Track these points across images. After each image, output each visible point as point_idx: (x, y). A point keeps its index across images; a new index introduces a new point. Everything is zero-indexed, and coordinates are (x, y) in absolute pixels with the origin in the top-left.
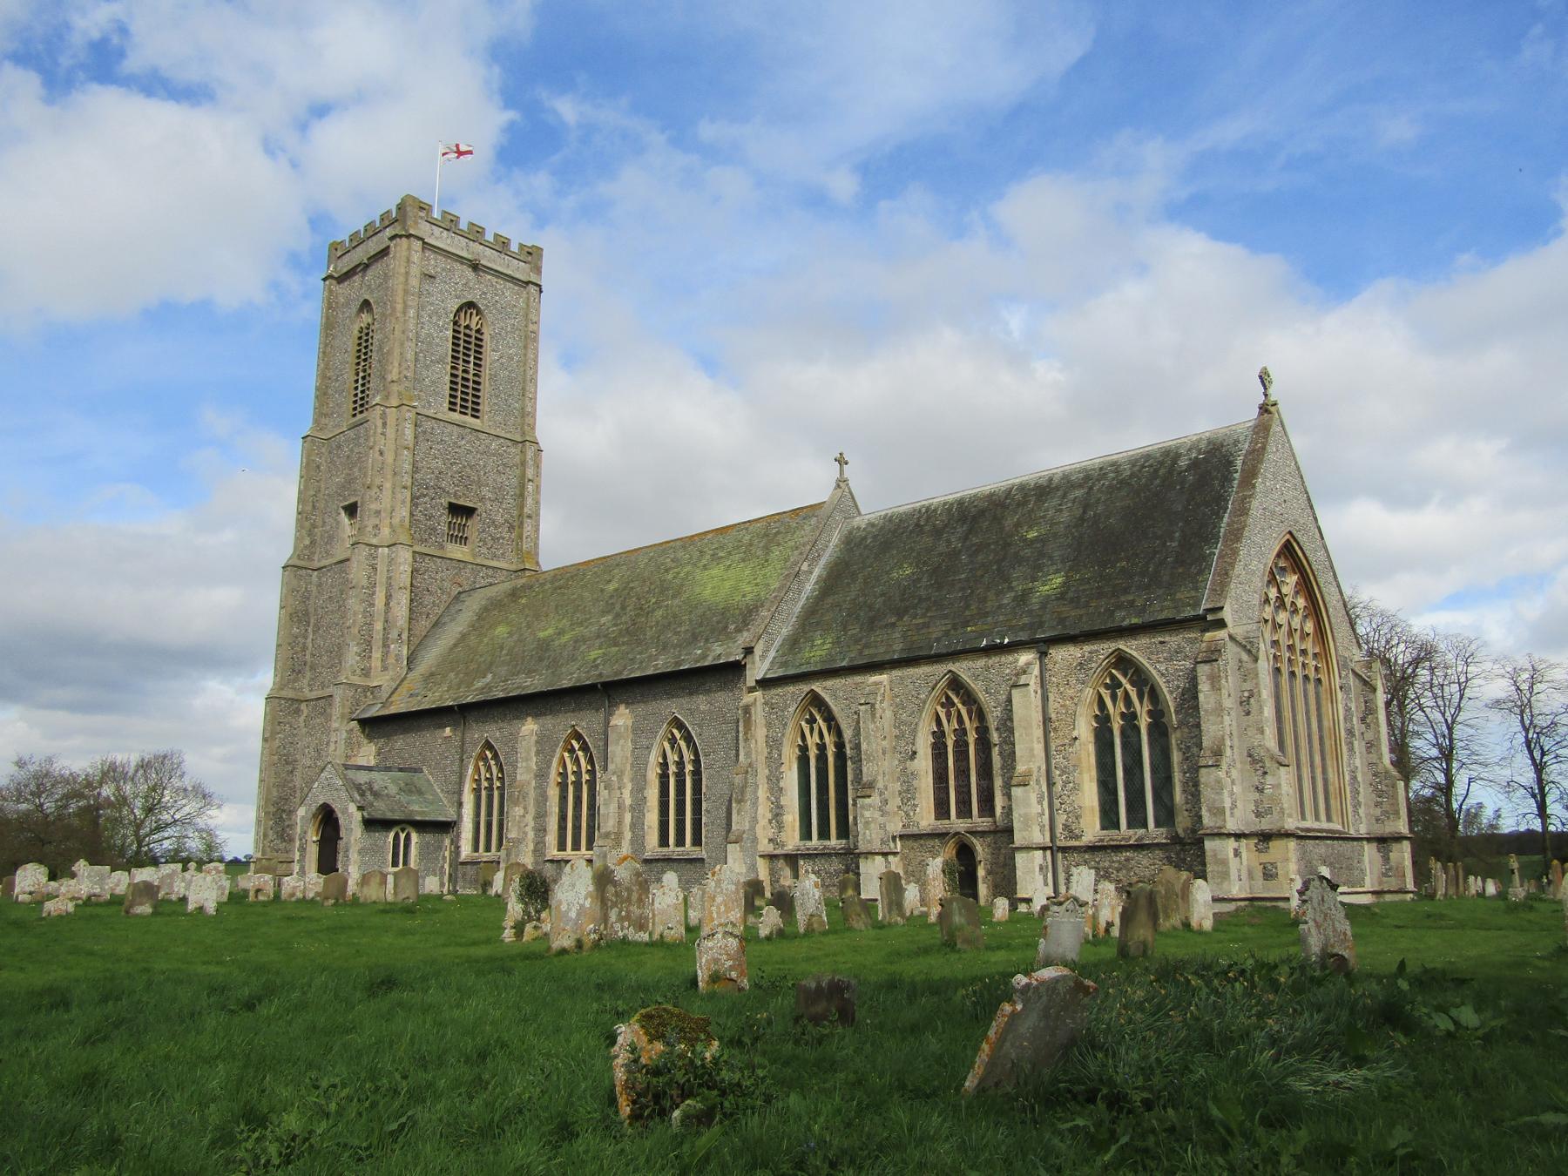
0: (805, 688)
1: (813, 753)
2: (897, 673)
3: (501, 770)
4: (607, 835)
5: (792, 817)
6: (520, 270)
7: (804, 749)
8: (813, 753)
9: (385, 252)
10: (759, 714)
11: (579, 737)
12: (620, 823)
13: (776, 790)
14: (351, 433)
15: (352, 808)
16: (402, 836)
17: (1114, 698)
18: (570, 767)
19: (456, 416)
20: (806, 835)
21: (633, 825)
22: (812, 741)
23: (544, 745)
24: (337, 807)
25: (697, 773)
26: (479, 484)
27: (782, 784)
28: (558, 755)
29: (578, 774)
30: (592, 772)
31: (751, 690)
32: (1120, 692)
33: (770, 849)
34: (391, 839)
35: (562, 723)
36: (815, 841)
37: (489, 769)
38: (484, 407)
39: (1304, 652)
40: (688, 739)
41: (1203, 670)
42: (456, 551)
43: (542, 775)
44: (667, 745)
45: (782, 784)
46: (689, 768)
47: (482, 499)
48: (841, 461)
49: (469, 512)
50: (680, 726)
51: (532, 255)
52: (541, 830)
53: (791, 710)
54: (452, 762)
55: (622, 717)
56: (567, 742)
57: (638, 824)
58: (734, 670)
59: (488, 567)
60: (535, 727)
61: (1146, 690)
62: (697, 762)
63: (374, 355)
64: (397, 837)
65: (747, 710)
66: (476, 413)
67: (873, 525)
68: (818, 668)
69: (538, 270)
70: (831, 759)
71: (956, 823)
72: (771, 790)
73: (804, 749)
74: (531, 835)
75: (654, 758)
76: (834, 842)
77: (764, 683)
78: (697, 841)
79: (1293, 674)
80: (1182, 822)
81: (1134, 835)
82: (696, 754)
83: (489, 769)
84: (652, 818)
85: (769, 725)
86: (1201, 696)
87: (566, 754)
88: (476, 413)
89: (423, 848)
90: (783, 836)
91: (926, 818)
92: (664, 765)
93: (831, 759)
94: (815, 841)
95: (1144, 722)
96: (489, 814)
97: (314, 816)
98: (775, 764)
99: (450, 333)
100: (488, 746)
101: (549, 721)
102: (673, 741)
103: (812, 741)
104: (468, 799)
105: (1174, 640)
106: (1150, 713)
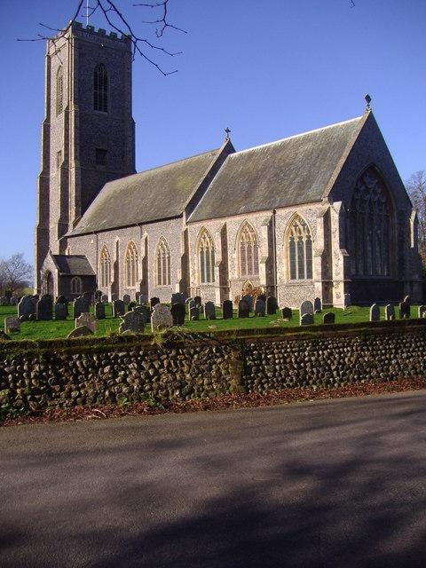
15: (57, 271)
19: (97, 112)
20: (203, 281)
38: (109, 107)
42: (102, 167)
66: (106, 110)
78: (169, 283)
99: (92, 78)
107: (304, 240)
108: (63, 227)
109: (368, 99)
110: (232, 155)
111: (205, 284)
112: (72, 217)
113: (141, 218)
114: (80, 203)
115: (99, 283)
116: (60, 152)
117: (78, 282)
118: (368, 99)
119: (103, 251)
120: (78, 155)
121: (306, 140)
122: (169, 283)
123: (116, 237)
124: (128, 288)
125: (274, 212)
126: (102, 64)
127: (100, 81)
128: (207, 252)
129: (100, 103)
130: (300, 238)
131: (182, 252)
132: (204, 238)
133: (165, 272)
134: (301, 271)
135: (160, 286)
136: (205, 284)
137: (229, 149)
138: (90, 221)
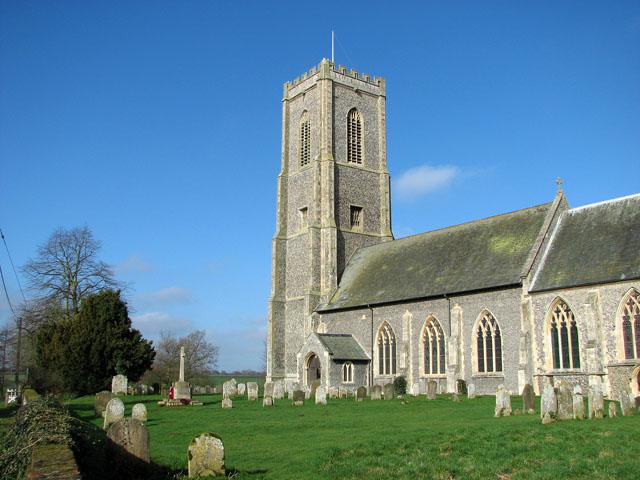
0: (554, 295)
1: (559, 327)
2: (604, 287)
4: (453, 366)
7: (554, 325)
8: (559, 327)
10: (531, 308)
12: (459, 360)
13: (541, 345)
15: (326, 354)
16: (348, 367)
18: (430, 334)
19: (351, 163)
20: (557, 365)
22: (559, 322)
23: (416, 323)
24: (318, 353)
25: (498, 336)
30: (442, 337)
31: (525, 296)
33: (537, 372)
36: (562, 369)
37: (386, 335)
38: (363, 158)
40: (493, 321)
43: (416, 338)
46: (493, 335)
49: (359, 209)
52: (416, 364)
56: (428, 322)
58: (519, 285)
65: (525, 306)
68: (561, 285)
70: (559, 331)
73: (554, 325)
74: (411, 366)
75: (475, 330)
76: (571, 369)
83: (386, 335)
84: (475, 358)
85: (536, 314)
87: (428, 329)
89: (357, 372)
90: (545, 367)
92: (480, 333)
93: (559, 331)
94: (562, 369)
96: (388, 356)
97: (306, 357)
98: (539, 331)
100: (386, 324)
101: (418, 313)
102: (484, 322)
103: (559, 322)
108: (315, 298)
113: (448, 288)
114: (336, 271)
116: (304, 210)
122: (499, 368)
123: (407, 314)
126: (354, 109)
128: (564, 329)
129: (353, 153)
135: (482, 373)
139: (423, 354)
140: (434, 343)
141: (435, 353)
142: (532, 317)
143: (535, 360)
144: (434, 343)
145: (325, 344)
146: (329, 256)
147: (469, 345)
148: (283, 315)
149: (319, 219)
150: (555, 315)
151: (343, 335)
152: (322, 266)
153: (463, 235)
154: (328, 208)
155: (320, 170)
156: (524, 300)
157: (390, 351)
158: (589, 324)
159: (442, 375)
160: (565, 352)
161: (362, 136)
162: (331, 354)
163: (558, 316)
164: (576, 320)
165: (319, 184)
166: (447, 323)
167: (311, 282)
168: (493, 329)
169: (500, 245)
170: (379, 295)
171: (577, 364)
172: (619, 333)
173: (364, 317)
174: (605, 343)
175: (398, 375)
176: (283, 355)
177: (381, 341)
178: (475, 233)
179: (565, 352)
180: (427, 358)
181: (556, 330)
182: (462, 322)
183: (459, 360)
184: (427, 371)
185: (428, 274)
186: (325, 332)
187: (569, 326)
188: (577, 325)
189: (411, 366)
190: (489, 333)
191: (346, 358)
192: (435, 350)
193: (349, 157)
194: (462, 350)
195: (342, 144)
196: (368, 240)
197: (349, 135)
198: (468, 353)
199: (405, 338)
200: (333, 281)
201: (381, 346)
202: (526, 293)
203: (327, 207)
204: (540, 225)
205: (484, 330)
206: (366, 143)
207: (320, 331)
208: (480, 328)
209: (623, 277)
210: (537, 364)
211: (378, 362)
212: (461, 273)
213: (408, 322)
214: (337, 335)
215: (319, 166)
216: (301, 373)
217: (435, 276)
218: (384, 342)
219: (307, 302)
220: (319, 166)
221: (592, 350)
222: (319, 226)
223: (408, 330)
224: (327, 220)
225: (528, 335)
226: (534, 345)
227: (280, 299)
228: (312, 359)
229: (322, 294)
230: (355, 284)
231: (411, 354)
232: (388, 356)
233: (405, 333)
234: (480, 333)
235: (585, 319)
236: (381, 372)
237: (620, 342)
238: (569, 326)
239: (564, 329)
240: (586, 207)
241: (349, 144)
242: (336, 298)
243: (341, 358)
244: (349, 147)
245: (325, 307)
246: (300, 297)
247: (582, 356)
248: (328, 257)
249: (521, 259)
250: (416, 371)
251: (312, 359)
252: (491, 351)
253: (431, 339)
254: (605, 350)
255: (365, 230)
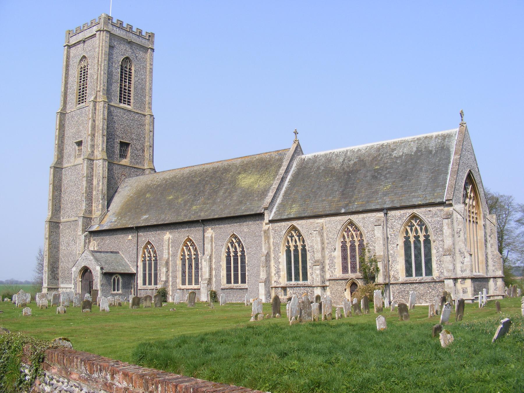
0: (290, 223)
1: (292, 249)
3: (155, 252)
5: (284, 273)
6: (144, 42)
8: (292, 249)
9: (94, 36)
11: (190, 240)
14: (78, 112)
17: (411, 230)
18: (186, 253)
19: (122, 105)
20: (289, 279)
21: (216, 276)
22: (292, 244)
24: (91, 267)
26: (131, 133)
27: (280, 260)
28: (181, 248)
29: (190, 255)
30: (196, 255)
31: (266, 224)
32: (414, 228)
33: (274, 284)
34: (112, 280)
35: (183, 234)
38: (132, 101)
39: (473, 212)
40: (239, 242)
41: (446, 221)
44: (230, 245)
45: (280, 260)
46: (239, 254)
47: (132, 139)
48: (296, 133)
49: (127, 145)
50: (236, 237)
51: (151, 36)
52: (175, 277)
53: (284, 232)
54: (133, 250)
55: (210, 232)
57: (218, 275)
59: (135, 168)
60: (171, 237)
61: (423, 227)
62: (243, 251)
63: (88, 79)
64: (114, 280)
66: (129, 103)
67: (310, 159)
68: (295, 216)
69: (153, 43)
71: (350, 275)
72: (275, 263)
77: (271, 221)
79: (470, 221)
80: (436, 274)
81: (418, 279)
82: (243, 248)
83: (149, 253)
84: (224, 273)
85: (274, 238)
86: (444, 231)
87: (185, 248)
88: (129, 103)
90: (281, 280)
91: (338, 273)
92: (229, 253)
95: (422, 239)
96: (150, 270)
97: (80, 271)
98: (277, 252)
99: (119, 70)
100: (149, 243)
101: (177, 235)
102: (232, 243)
103: (292, 244)
104: (140, 264)
105: (434, 209)
106: (425, 236)
107: (422, 239)
109: (462, 114)
110: (303, 157)
111: (293, 282)
112: (97, 213)
113: (203, 215)
114: (106, 197)
115: (140, 281)
116: (79, 144)
117: (118, 280)
118: (462, 114)
119: (146, 247)
120: (105, 146)
121: (398, 145)
122: (243, 281)
124: (183, 287)
125: (386, 214)
126: (127, 58)
127: (125, 74)
128: (296, 250)
129: (124, 97)
130: (417, 238)
131: (264, 251)
132: (292, 236)
133: (150, 275)
134: (236, 276)
135: (229, 285)
136: (293, 282)
137: (298, 150)
138: (121, 214)
139: (181, 269)
140: (190, 259)
141: (191, 268)
142: (272, 240)
143: (273, 274)
144: (190, 259)
145: (97, 260)
146: (101, 184)
147: (219, 262)
148: (58, 234)
149: (93, 152)
150: (289, 239)
151: (112, 252)
152: (94, 193)
153: (216, 171)
154: (100, 142)
155: (95, 109)
156: (265, 227)
157: (152, 266)
158: (315, 247)
159: (196, 287)
160: (297, 269)
161: (132, 82)
162: (102, 269)
163: (292, 240)
164: (306, 243)
165: (94, 121)
166: (201, 243)
167: (84, 206)
168: (239, 249)
169: (246, 181)
170: (144, 219)
171: (305, 278)
172: (338, 254)
173: (130, 236)
174: (327, 262)
175: (159, 286)
176: (58, 268)
177: (144, 257)
178: (226, 170)
179: (297, 269)
180: (184, 272)
181: (355, 246)
182: (213, 243)
183: (211, 274)
184: (184, 283)
185: (186, 202)
186: (96, 249)
187: (300, 248)
188: (307, 248)
189: (170, 279)
190: (236, 252)
191: (114, 271)
192: (190, 266)
193: (120, 100)
194: (214, 266)
195: (116, 88)
196: (136, 170)
197: (121, 80)
198: (218, 269)
199: (165, 256)
200: (103, 206)
201: (144, 262)
202: (268, 222)
203: (100, 141)
204: (280, 166)
205: (232, 250)
206: (135, 88)
207: (92, 249)
208: (229, 249)
209: (343, 211)
210: (274, 278)
211: (142, 275)
212: (214, 203)
213: (167, 241)
214: (107, 252)
215: (95, 106)
216: (75, 284)
217: (191, 206)
218: (148, 259)
219: (80, 223)
220: (95, 106)
221: (318, 267)
222: (92, 158)
223: (169, 249)
224: (100, 153)
225: (268, 255)
226: (272, 263)
227: (55, 220)
228: (85, 271)
229: (94, 216)
230: (122, 208)
231: (171, 269)
232: (150, 270)
233: (165, 252)
234: (229, 253)
235: (313, 243)
236: (144, 283)
237: (339, 261)
238: (300, 248)
239: (296, 250)
240: (316, 154)
241: (121, 88)
242: (106, 219)
243: (111, 271)
244: (121, 91)
245: (95, 228)
246: (73, 219)
247: (309, 271)
248: (100, 185)
249: (264, 193)
250: (174, 283)
251: (85, 271)
252: (236, 267)
253: (232, 254)
254: (327, 267)
255: (131, 162)
